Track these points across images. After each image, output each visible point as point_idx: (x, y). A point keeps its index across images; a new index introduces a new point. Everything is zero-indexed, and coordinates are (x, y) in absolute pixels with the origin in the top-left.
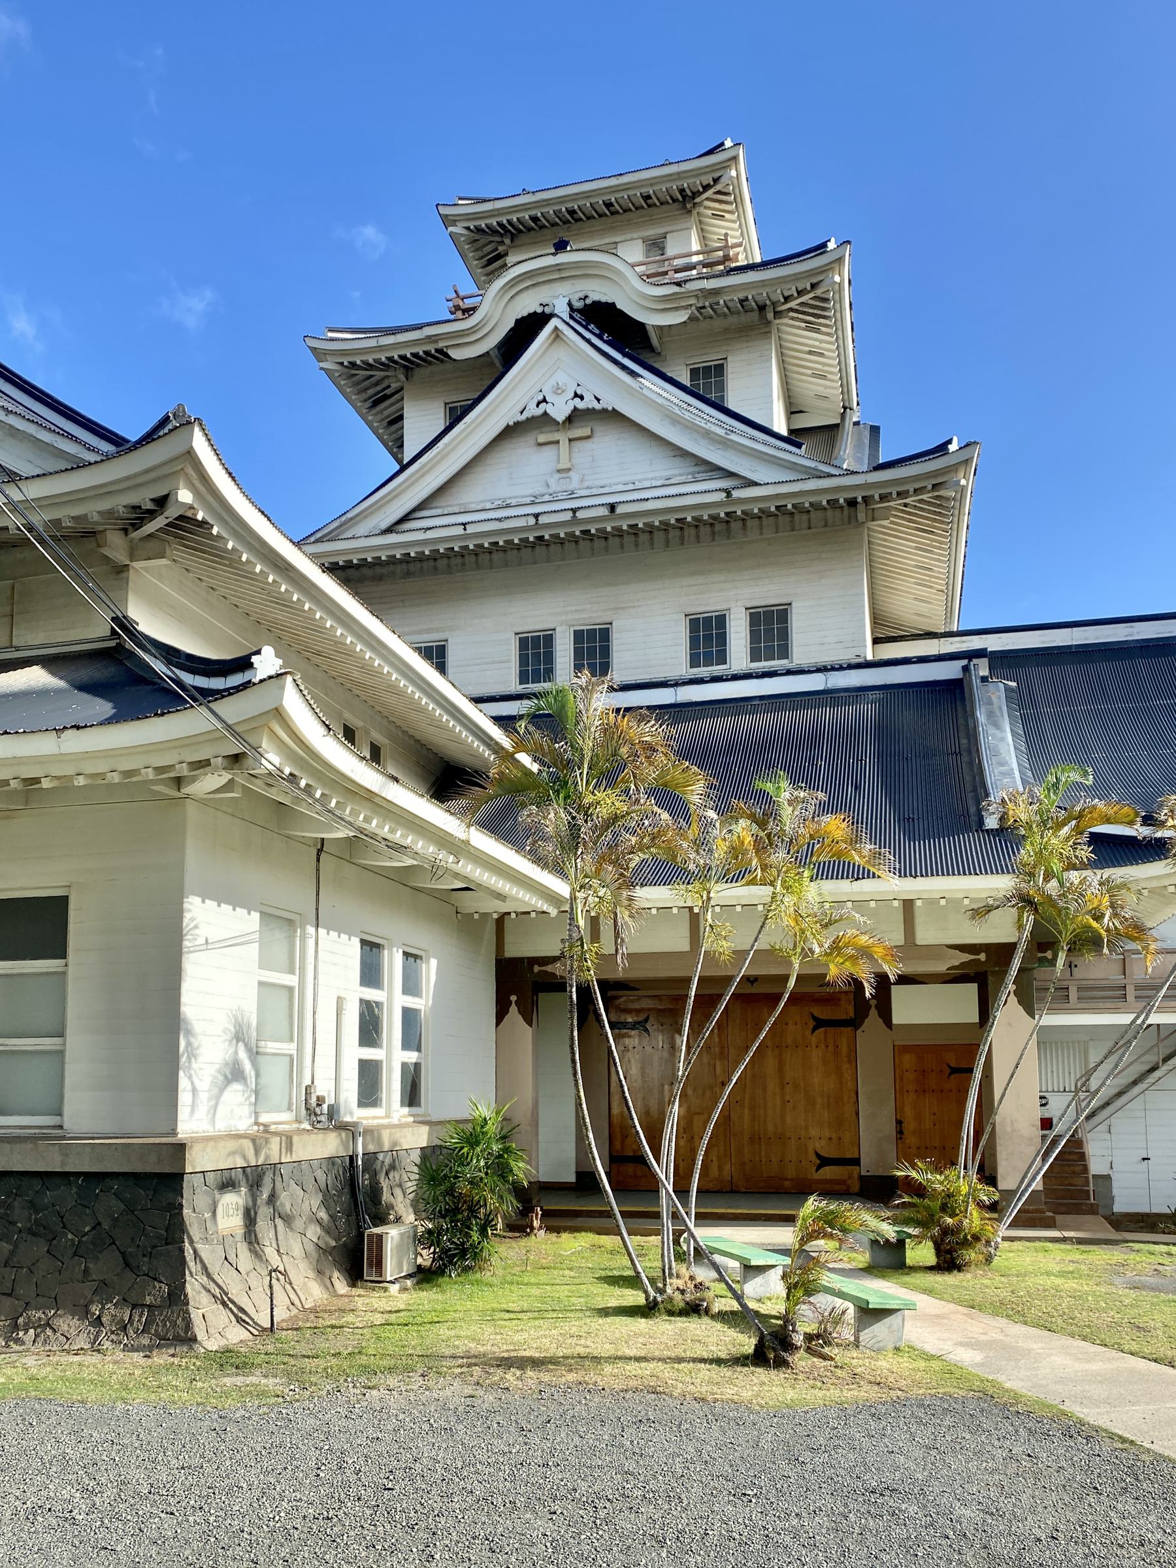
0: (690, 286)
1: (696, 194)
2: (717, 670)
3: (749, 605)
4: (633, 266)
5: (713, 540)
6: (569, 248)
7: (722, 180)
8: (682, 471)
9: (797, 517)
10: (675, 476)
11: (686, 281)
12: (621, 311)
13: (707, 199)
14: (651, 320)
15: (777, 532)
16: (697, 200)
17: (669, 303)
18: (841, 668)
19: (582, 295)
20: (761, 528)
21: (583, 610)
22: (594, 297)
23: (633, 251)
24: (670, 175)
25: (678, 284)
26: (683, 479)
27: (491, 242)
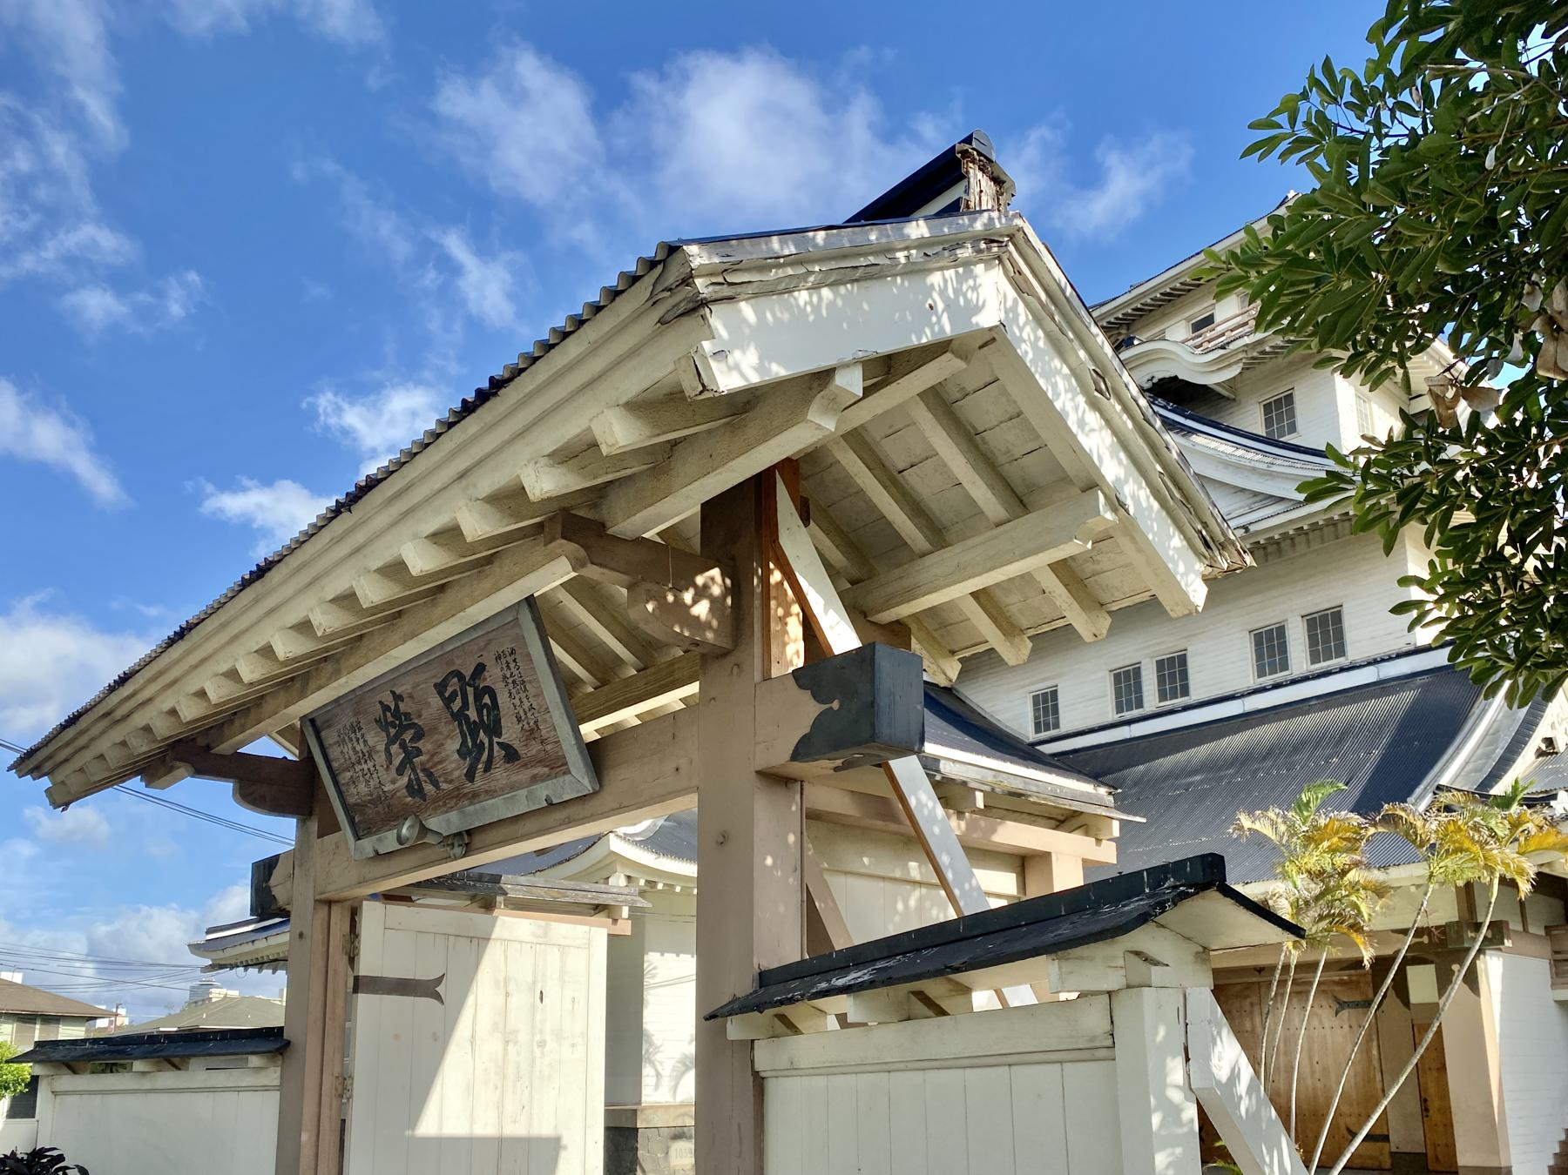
0: (1232, 347)
2: (1280, 676)
3: (1303, 613)
4: (1183, 342)
5: (1267, 561)
6: (1136, 342)
9: (1340, 526)
11: (1228, 343)
12: (1183, 380)
14: (1211, 380)
15: (1323, 543)
18: (1390, 659)
19: (1149, 377)
20: (1308, 542)
21: (1162, 642)
22: (1159, 375)
23: (1178, 330)
25: (1223, 347)
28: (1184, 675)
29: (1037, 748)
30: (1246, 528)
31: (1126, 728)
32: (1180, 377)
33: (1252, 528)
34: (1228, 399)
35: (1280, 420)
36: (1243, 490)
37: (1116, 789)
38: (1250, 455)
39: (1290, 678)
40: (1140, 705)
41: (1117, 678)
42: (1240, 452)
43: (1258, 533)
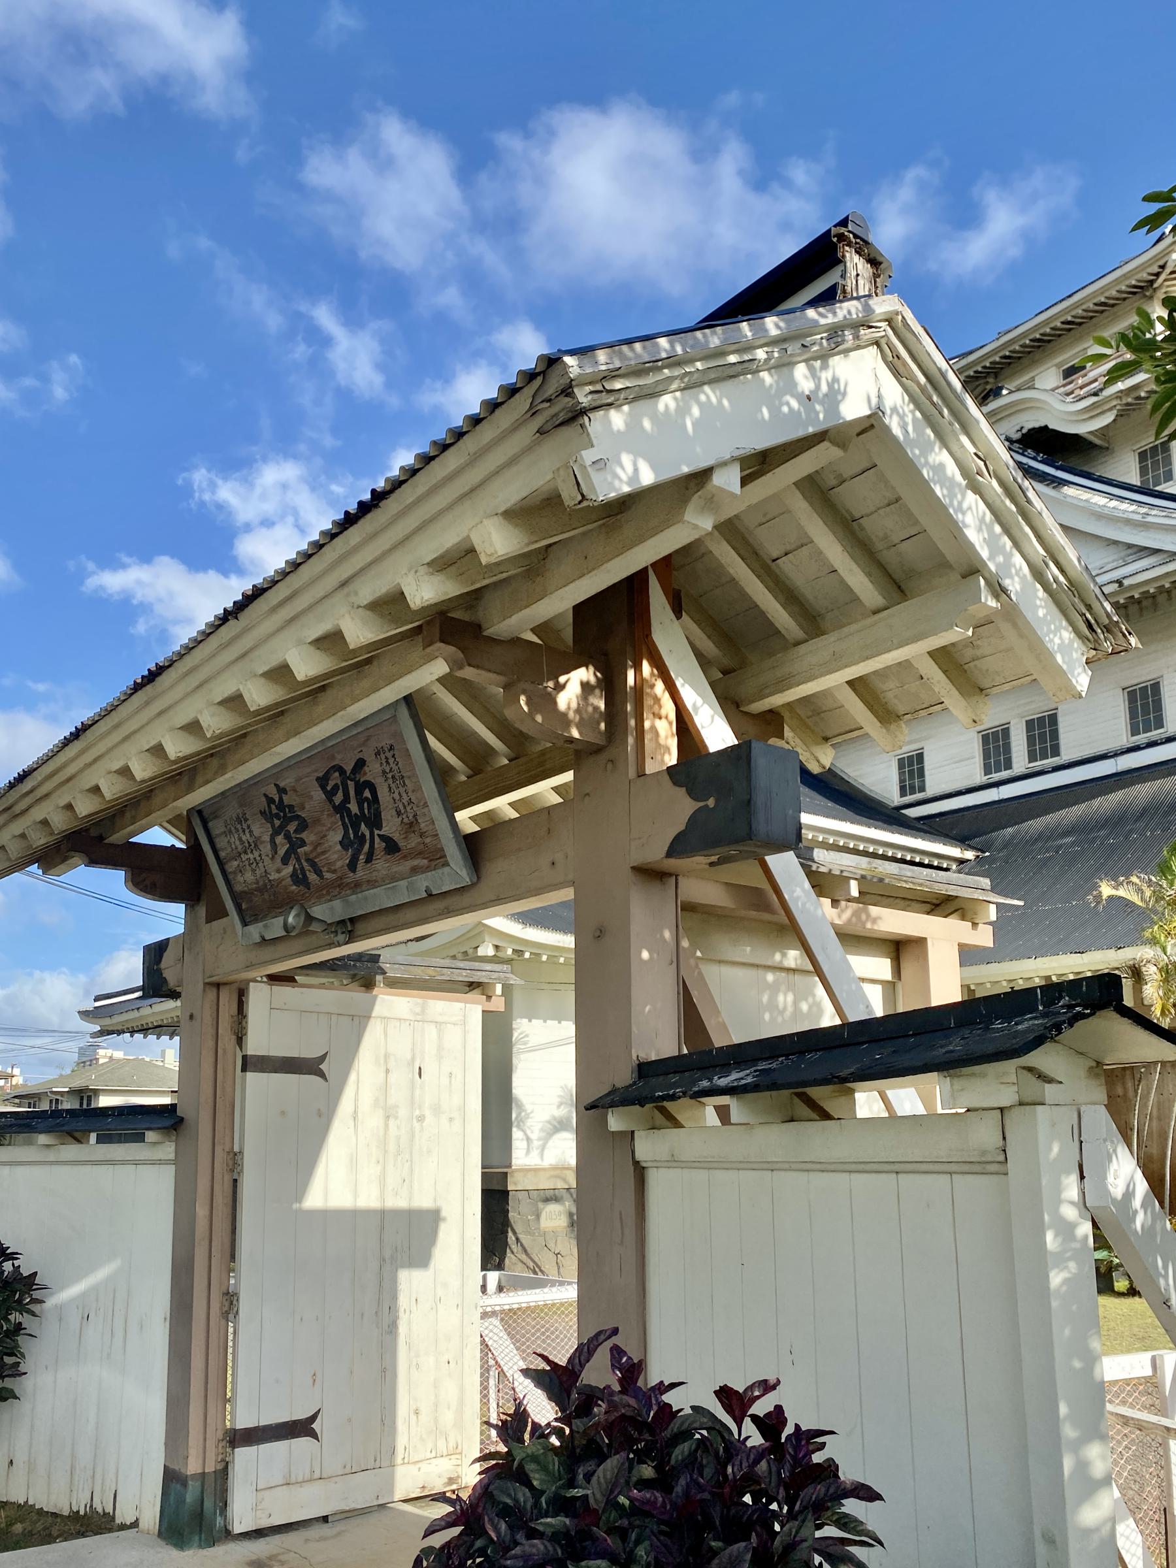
1: (1152, 282)
2: (1154, 734)
4: (1053, 390)
7: (1168, 264)
8: (1115, 557)
10: (1109, 563)
13: (1165, 280)
14: (1082, 429)
16: (1155, 285)
17: (1092, 412)
19: (1018, 428)
22: (1029, 425)
23: (1048, 377)
24: (1116, 279)
25: (1095, 394)
26: (1115, 564)
27: (978, 386)
28: (1055, 735)
29: (903, 811)
30: (1119, 582)
31: (994, 790)
32: (1051, 427)
33: (1126, 582)
34: (1100, 447)
35: (1156, 465)
36: (1116, 543)
37: (984, 852)
38: (1125, 506)
39: (1167, 735)
40: (1008, 766)
41: (985, 739)
42: (1114, 503)
43: (1132, 587)
